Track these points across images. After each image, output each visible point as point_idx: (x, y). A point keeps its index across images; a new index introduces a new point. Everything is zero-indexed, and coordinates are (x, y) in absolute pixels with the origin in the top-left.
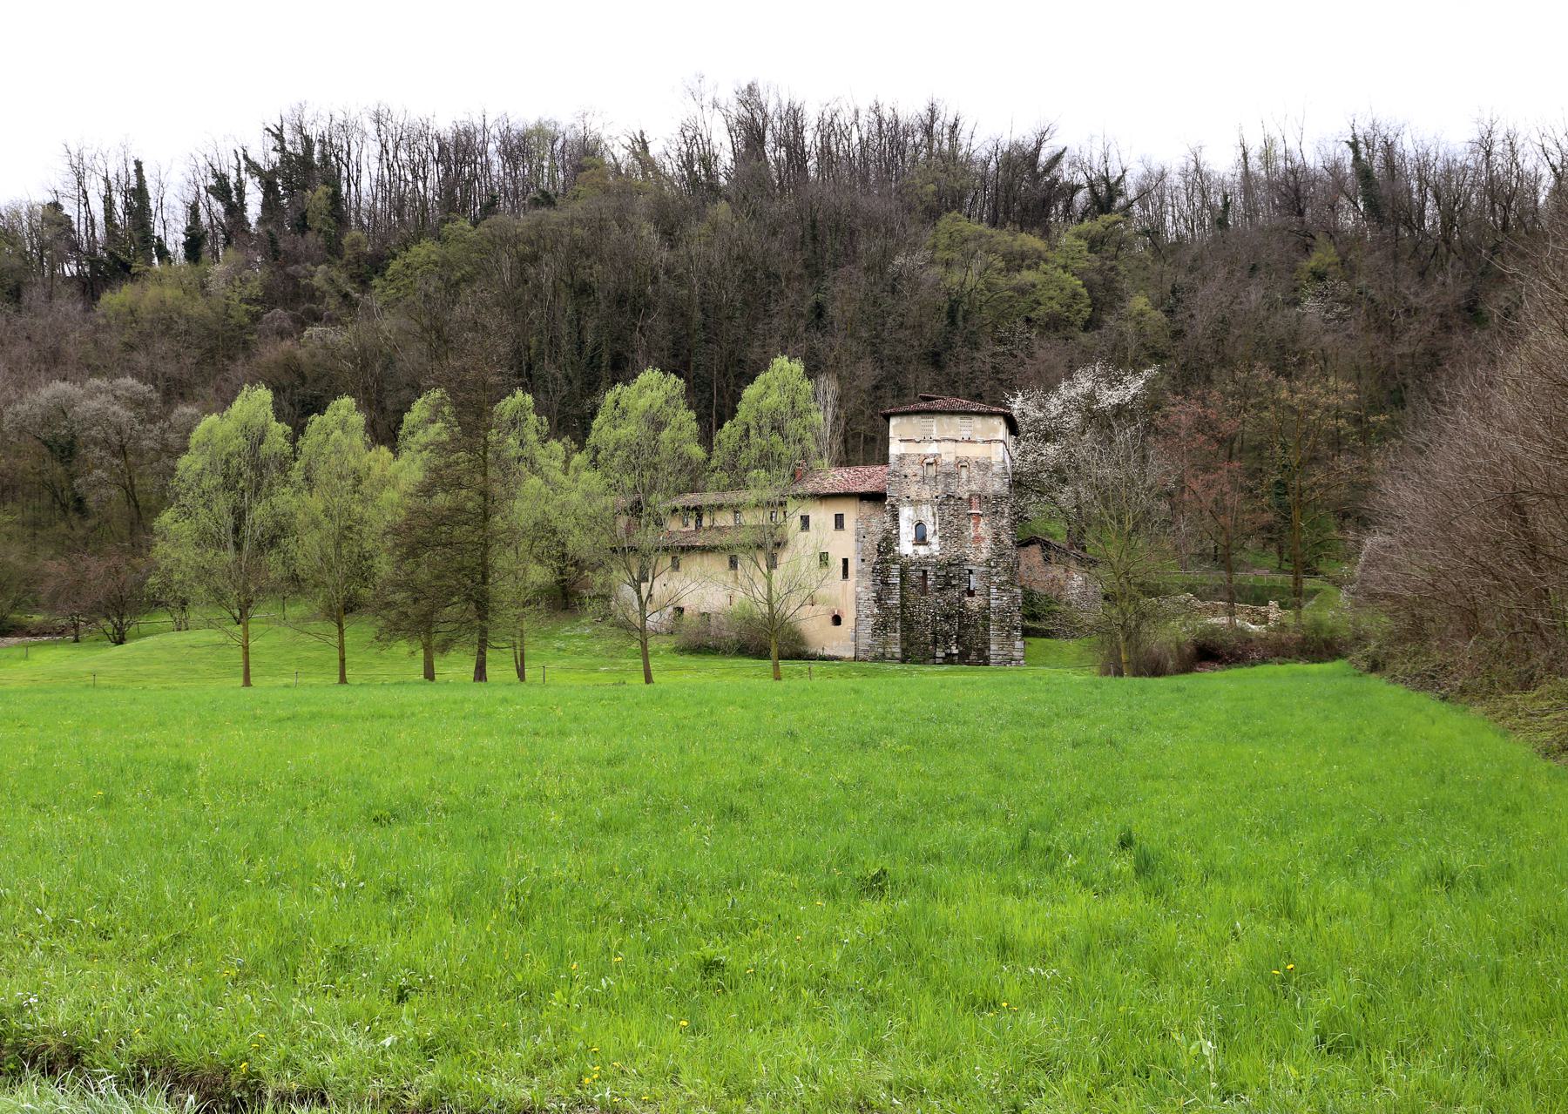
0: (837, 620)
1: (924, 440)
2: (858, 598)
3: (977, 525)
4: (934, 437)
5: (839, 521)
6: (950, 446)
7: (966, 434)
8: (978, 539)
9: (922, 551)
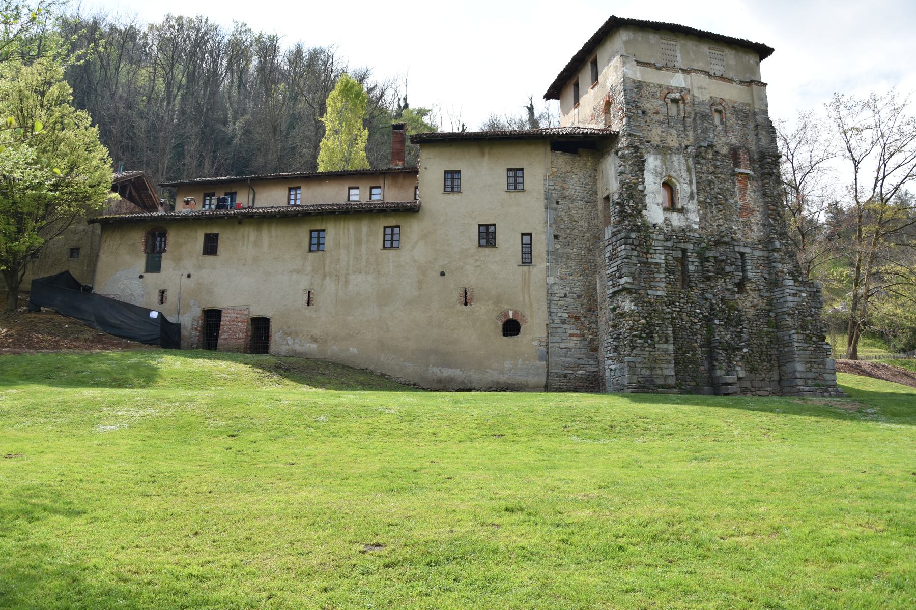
0: (511, 328)
1: (666, 67)
2: (550, 294)
3: (743, 190)
4: (679, 64)
5: (515, 179)
6: (702, 79)
7: (717, 69)
8: (746, 210)
9: (676, 220)
